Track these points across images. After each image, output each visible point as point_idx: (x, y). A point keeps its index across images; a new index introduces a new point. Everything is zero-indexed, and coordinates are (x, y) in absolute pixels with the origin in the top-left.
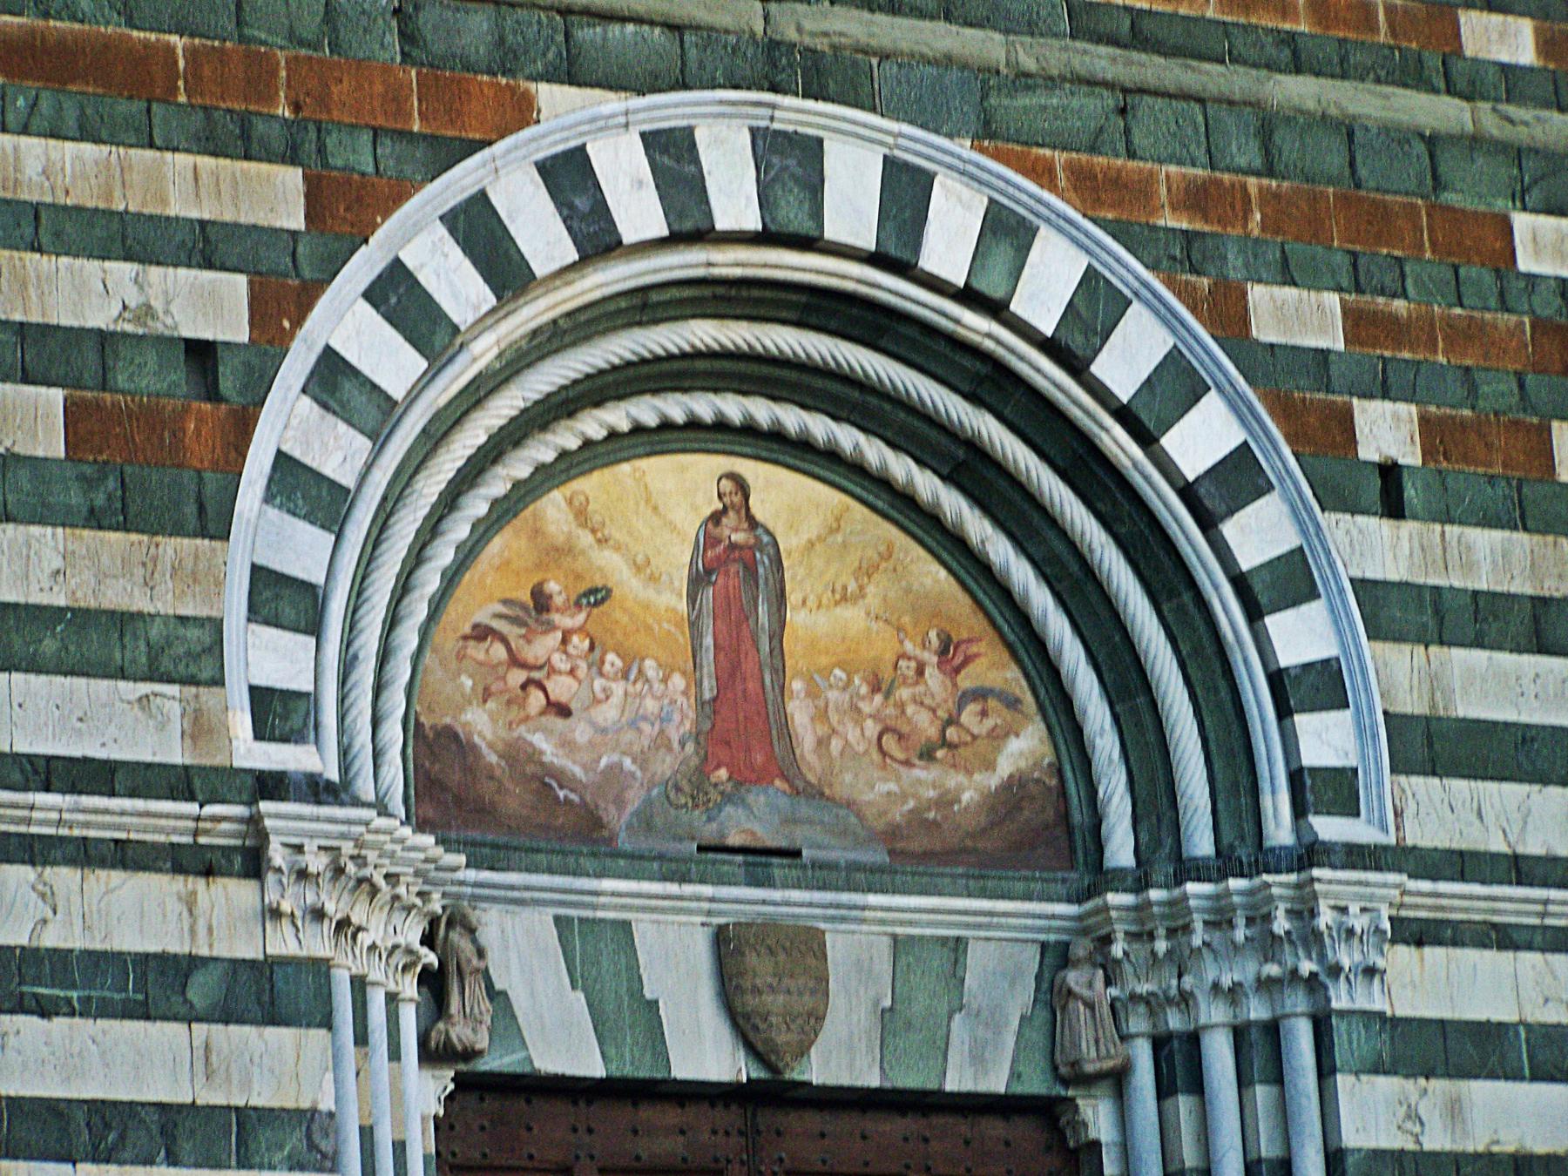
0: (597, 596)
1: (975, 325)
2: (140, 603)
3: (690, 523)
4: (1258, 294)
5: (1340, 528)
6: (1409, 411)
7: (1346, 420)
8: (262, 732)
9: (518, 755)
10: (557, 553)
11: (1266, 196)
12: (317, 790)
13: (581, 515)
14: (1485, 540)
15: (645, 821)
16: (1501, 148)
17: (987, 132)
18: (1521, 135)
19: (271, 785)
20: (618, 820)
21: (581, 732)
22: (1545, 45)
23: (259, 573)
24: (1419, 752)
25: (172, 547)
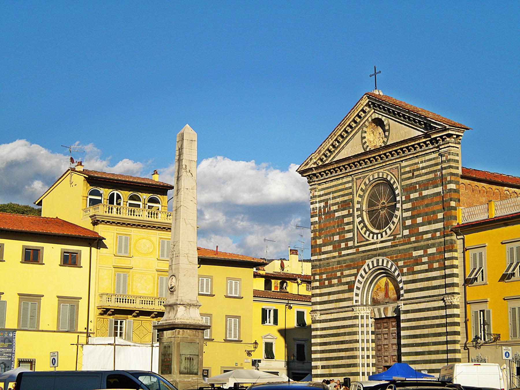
0: (380, 288)
1: (387, 268)
2: (350, 297)
3: (385, 282)
4: (399, 262)
5: (402, 277)
6: (406, 268)
7: (403, 270)
8: (356, 303)
9: (377, 299)
10: (379, 286)
11: (400, 255)
12: (359, 306)
13: (380, 283)
14: (410, 276)
15: (382, 301)
16: (412, 247)
17: (386, 256)
18: (413, 246)
19: (354, 306)
20: (381, 302)
21: (379, 296)
22: (415, 239)
23: (356, 293)
24: (406, 292)
25: (352, 293)
